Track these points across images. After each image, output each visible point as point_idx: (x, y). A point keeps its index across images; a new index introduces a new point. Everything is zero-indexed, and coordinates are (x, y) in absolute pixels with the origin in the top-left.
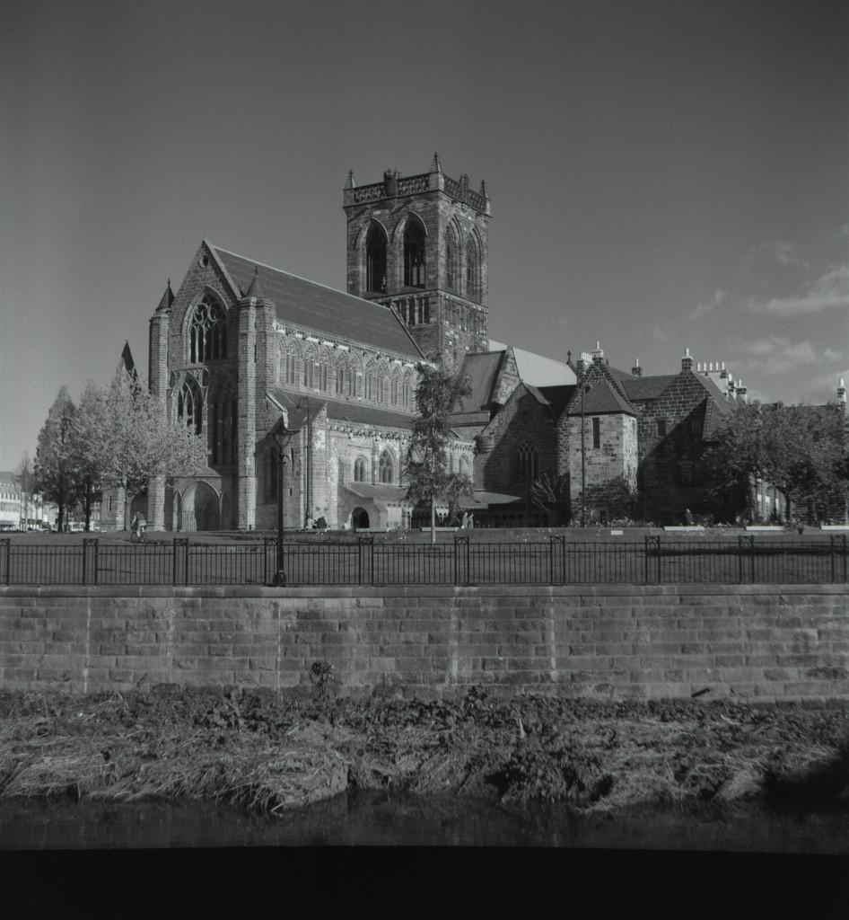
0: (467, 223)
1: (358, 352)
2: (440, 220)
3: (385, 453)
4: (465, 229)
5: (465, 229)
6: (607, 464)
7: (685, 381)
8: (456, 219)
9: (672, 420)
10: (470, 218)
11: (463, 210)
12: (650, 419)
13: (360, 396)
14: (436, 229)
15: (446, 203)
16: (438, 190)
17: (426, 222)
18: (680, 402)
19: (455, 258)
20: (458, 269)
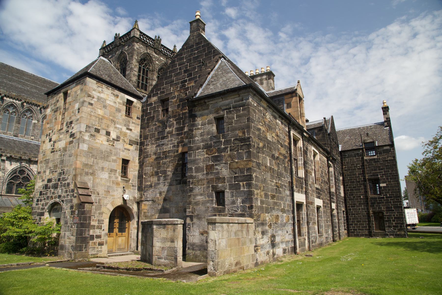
0: (161, 61)
1: (33, 107)
2: (135, 53)
3: (22, 171)
4: (157, 62)
5: (157, 62)
6: (65, 149)
7: (193, 46)
8: (148, 55)
9: (176, 94)
10: (161, 58)
11: (156, 53)
12: (154, 99)
13: (32, 136)
14: (132, 56)
15: (142, 46)
16: (134, 36)
17: (128, 54)
18: (185, 72)
19: (150, 75)
20: (151, 82)
